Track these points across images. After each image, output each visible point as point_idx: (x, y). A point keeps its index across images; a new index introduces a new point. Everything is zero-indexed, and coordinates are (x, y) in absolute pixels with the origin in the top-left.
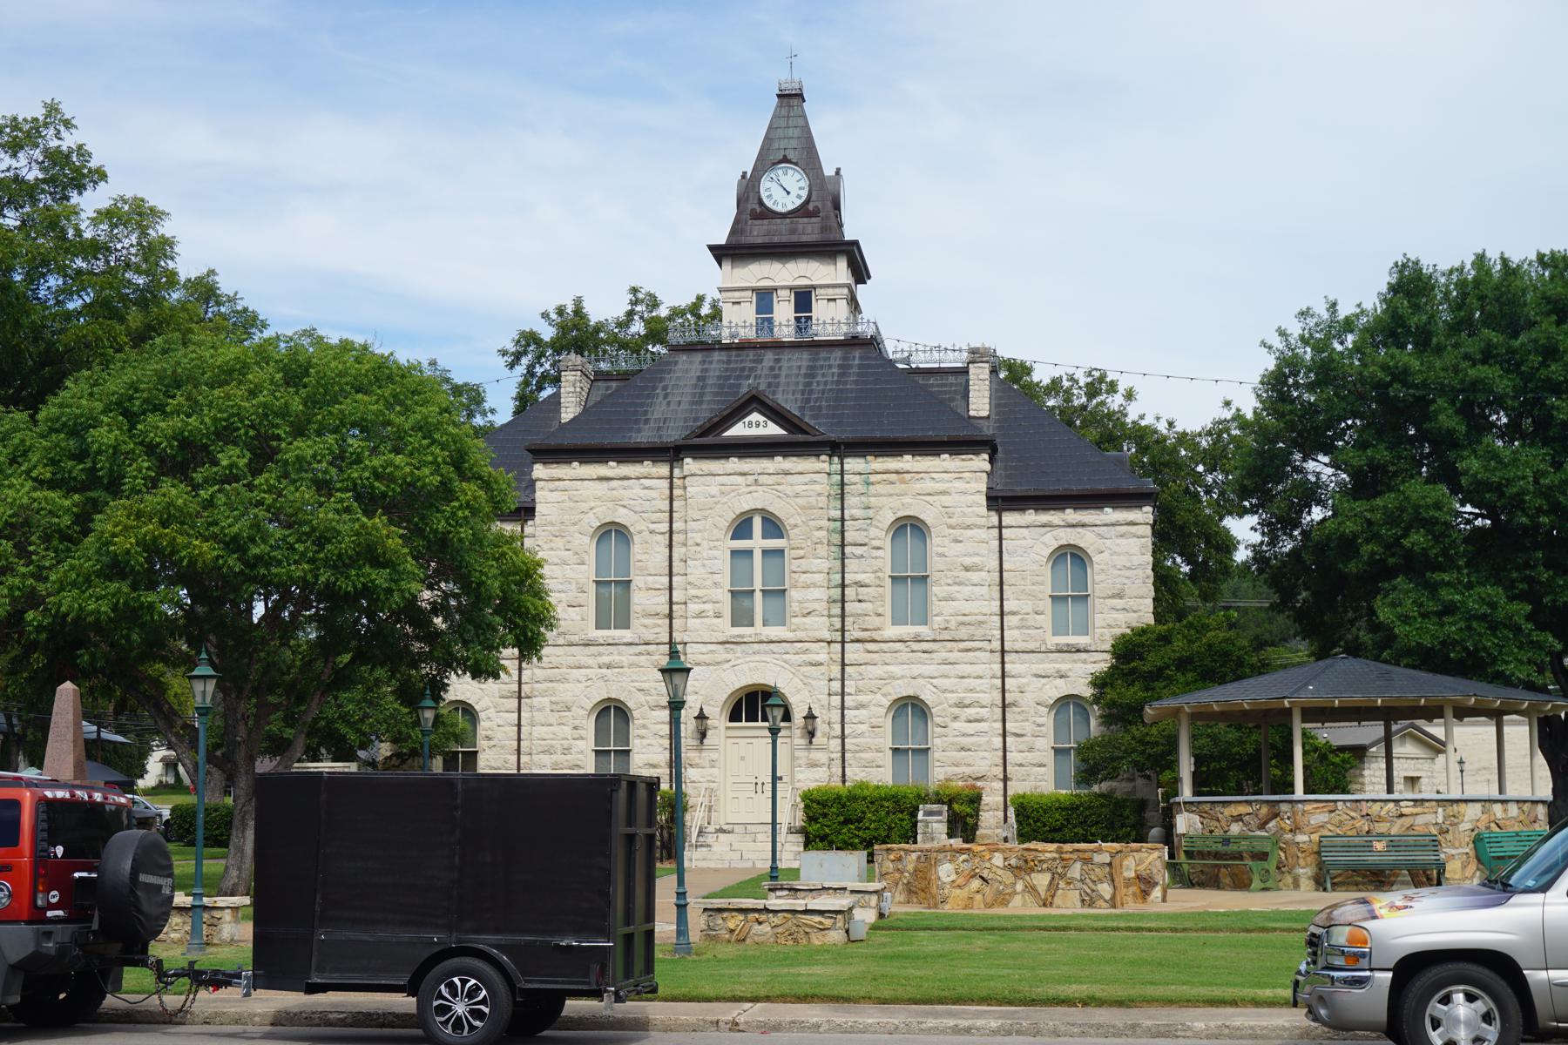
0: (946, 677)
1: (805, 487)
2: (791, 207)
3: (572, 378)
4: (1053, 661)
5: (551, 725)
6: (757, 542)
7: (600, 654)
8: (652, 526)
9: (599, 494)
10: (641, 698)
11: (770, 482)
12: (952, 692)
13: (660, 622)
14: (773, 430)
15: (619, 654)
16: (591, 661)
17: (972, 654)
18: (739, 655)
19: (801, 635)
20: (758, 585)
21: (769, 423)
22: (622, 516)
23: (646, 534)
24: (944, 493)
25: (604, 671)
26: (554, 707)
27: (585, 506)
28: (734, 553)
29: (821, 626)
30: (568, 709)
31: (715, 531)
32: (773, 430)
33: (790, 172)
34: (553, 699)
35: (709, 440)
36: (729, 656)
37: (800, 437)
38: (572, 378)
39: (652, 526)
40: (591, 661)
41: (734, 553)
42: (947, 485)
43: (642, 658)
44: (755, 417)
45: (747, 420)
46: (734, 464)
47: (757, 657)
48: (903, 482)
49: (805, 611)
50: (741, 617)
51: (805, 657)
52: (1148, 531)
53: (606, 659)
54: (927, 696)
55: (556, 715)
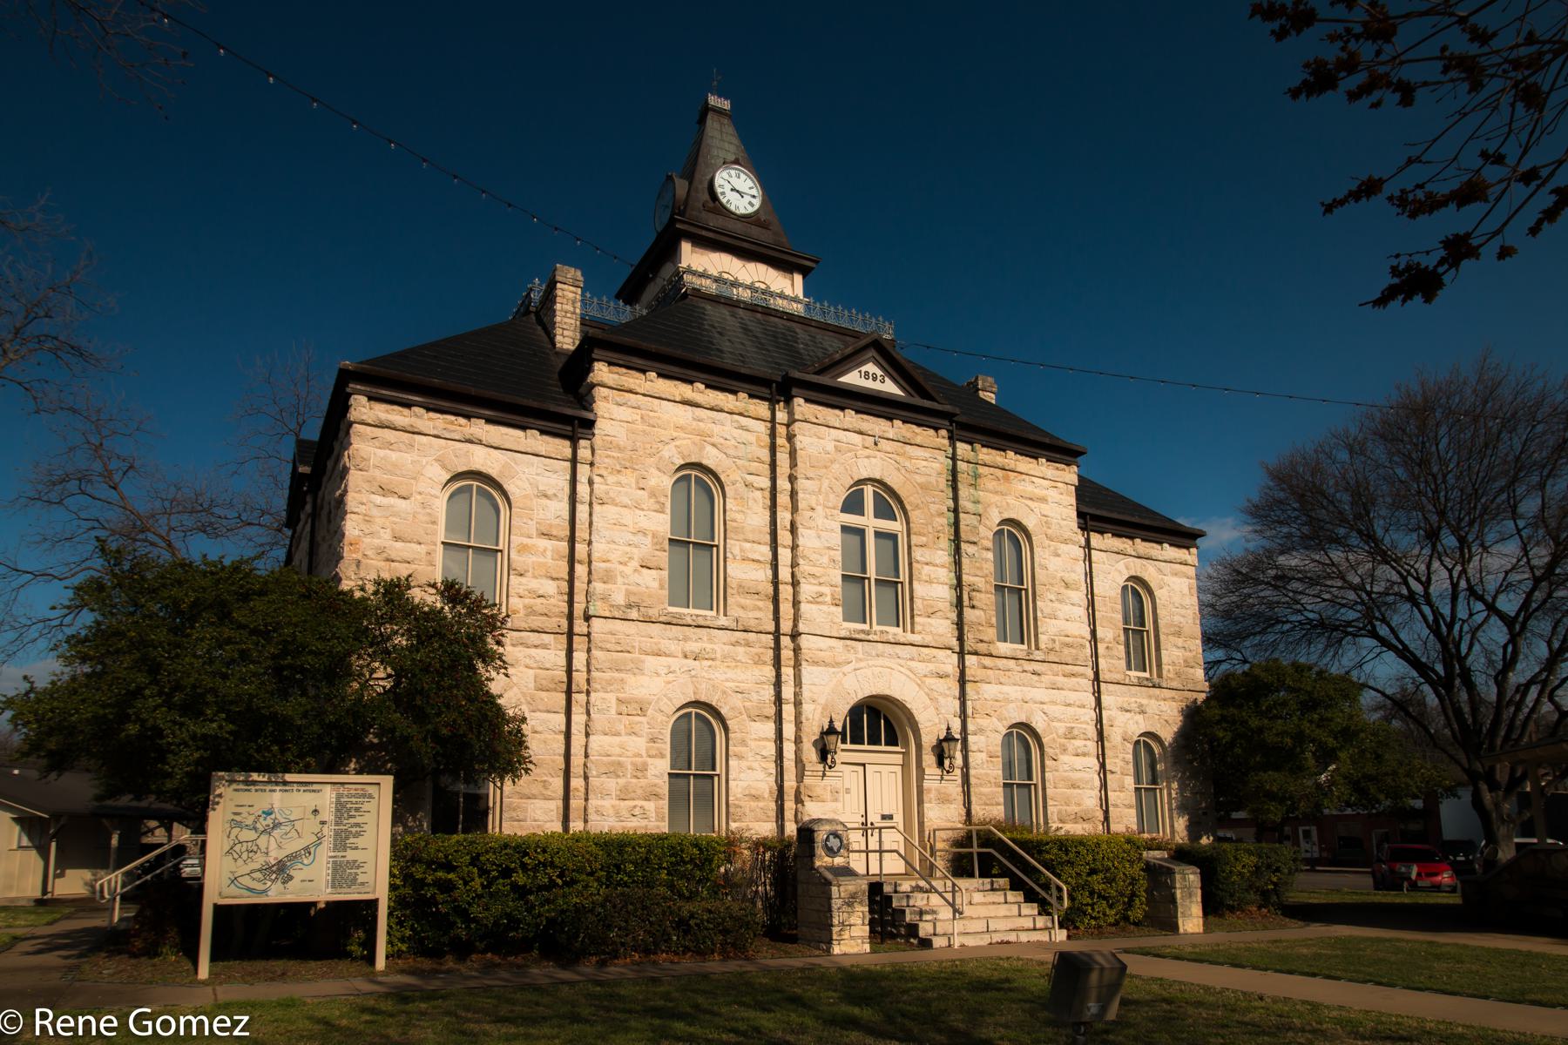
0: (1053, 703)
1: (925, 463)
2: (742, 211)
3: (571, 295)
4: (1135, 695)
5: (618, 734)
6: (870, 522)
7: (686, 639)
8: (750, 478)
9: (682, 422)
10: (737, 701)
11: (889, 449)
12: (1060, 721)
13: (761, 604)
14: (890, 387)
15: (710, 640)
16: (673, 647)
17: (1074, 680)
18: (860, 656)
19: (928, 640)
20: (872, 572)
21: (886, 379)
22: (711, 458)
23: (740, 486)
24: (1043, 500)
25: (690, 662)
26: (624, 709)
27: (665, 435)
28: (846, 529)
29: (943, 628)
30: (642, 711)
31: (832, 496)
32: (890, 387)
33: (743, 176)
34: (621, 696)
35: (824, 380)
36: (852, 657)
37: (927, 404)
38: (571, 295)
39: (750, 478)
40: (673, 647)
41: (846, 529)
42: (1045, 492)
43: (740, 649)
44: (871, 368)
45: (864, 369)
46: (850, 418)
47: (880, 661)
48: (1007, 479)
49: (931, 611)
50: (857, 612)
51: (931, 667)
52: (1191, 571)
53: (693, 646)
54: (1039, 724)
55: (625, 719)
